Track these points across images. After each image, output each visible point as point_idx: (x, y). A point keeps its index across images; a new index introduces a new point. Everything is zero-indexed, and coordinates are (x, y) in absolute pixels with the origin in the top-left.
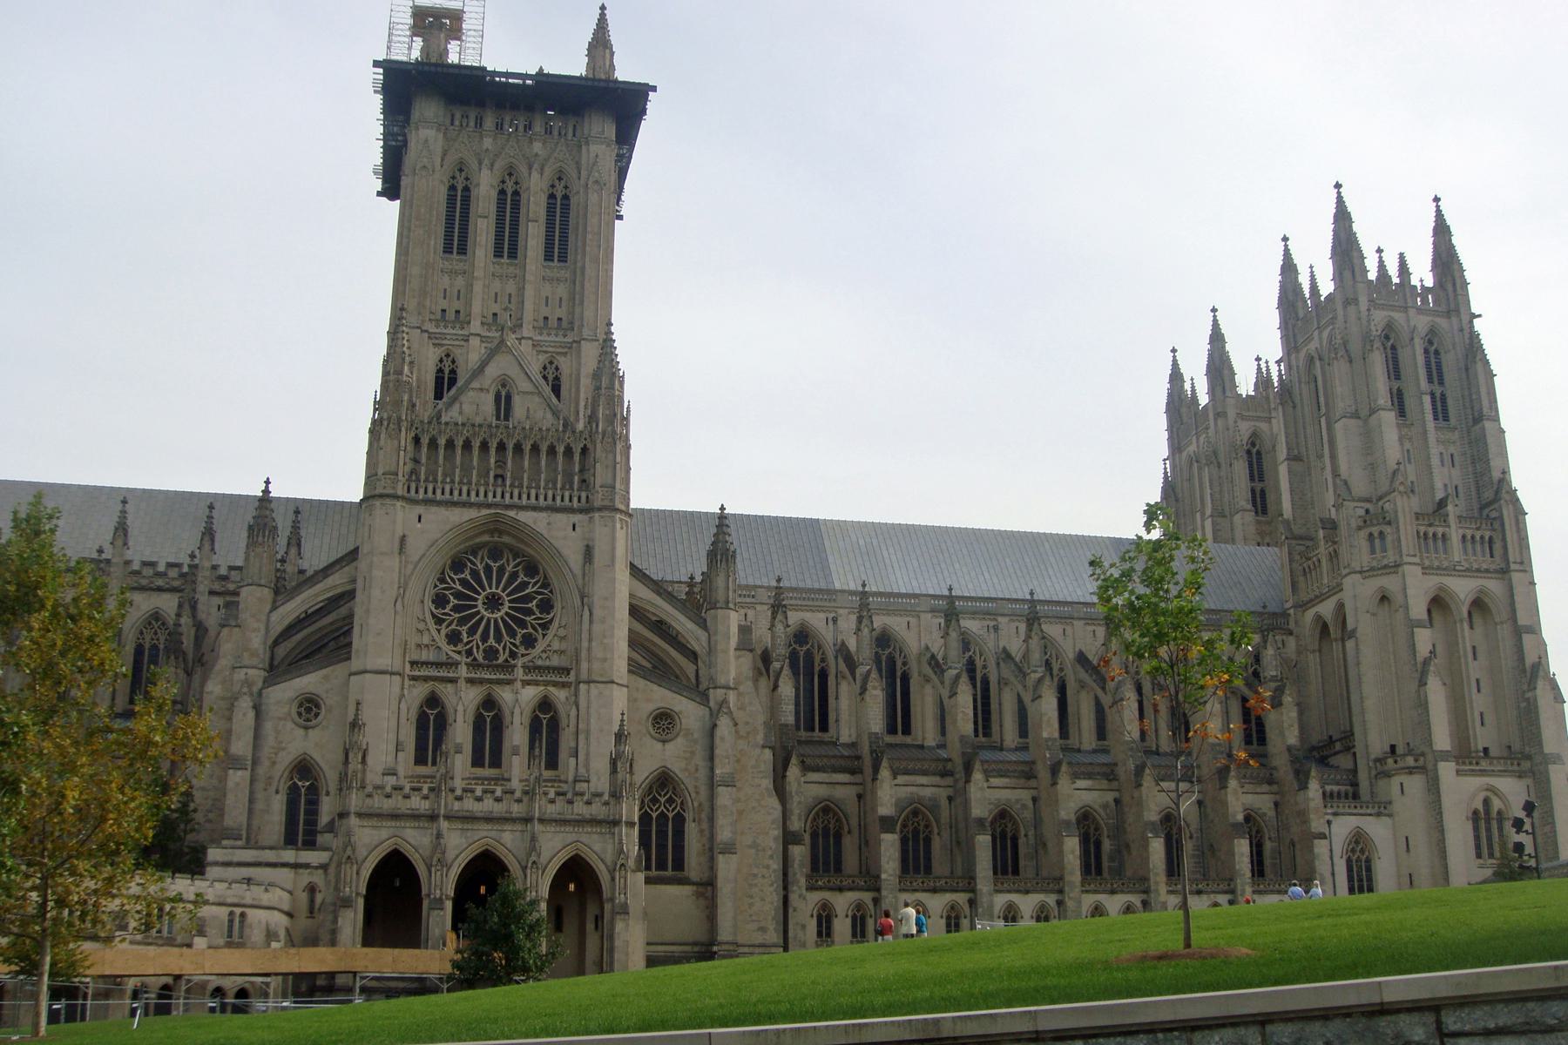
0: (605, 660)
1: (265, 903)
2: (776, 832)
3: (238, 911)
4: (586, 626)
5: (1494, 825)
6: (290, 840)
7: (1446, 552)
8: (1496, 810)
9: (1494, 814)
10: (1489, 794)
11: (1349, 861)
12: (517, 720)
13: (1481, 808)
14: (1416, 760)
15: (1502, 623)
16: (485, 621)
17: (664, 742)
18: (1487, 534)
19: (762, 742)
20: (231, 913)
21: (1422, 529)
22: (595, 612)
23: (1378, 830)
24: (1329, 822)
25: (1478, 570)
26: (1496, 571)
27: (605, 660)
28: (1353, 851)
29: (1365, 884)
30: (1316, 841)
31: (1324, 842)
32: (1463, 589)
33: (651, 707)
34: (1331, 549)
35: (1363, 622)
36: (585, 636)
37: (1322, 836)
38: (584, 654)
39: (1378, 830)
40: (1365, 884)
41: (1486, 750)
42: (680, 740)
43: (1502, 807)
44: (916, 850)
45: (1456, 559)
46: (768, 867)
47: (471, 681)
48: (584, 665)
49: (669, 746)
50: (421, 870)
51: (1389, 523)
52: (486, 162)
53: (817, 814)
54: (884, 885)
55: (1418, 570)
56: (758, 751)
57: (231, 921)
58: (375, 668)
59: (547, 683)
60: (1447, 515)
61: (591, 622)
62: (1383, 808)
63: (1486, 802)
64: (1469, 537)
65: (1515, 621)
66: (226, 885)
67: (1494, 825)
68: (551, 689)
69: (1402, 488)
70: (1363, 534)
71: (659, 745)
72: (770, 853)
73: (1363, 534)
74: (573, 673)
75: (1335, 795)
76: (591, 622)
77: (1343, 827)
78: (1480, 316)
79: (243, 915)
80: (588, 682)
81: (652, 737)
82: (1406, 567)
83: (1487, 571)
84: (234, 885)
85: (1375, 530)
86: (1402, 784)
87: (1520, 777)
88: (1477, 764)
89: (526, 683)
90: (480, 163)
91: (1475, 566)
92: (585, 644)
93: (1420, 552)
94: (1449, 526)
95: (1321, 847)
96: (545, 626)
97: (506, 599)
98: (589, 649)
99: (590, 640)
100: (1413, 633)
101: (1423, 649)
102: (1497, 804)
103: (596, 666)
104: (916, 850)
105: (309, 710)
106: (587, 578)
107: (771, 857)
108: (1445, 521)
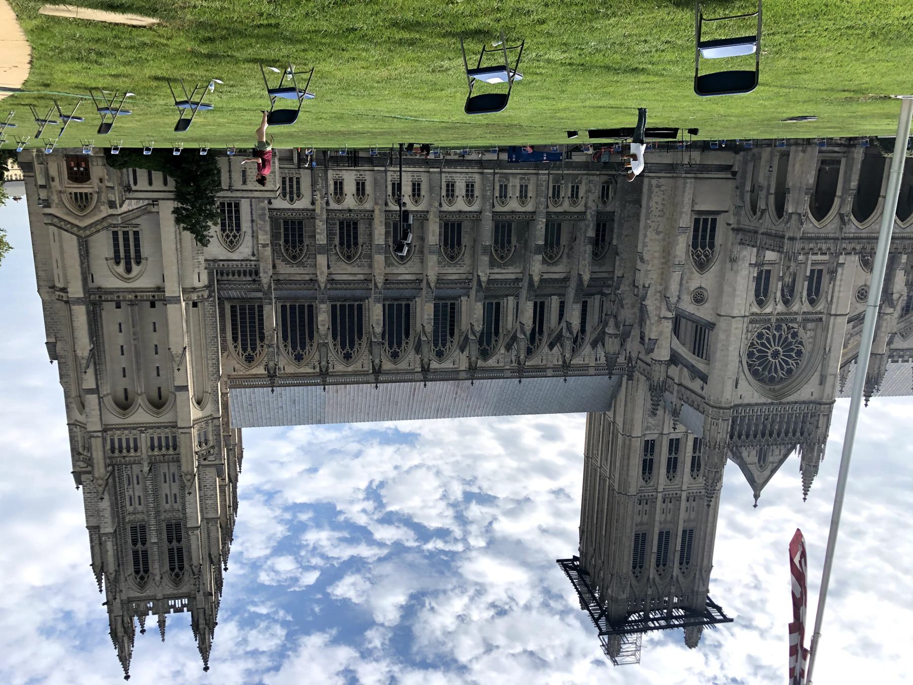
5: (122, 254)
9: (123, 262)
10: (126, 276)
11: (238, 230)
13: (134, 265)
15: (108, 394)
17: (701, 288)
21: (171, 452)
28: (235, 236)
32: (142, 415)
33: (707, 305)
41: (118, 307)
42: (692, 289)
43: (115, 267)
44: (503, 236)
47: (821, 313)
49: (698, 285)
52: (675, 579)
53: (556, 256)
54: (544, 215)
59: (761, 314)
63: (129, 270)
65: (99, 398)
67: (122, 254)
68: (759, 312)
71: (703, 286)
75: (248, 274)
80: (745, 316)
81: (706, 290)
89: (796, 313)
90: (677, 579)
104: (503, 236)
105: (862, 294)
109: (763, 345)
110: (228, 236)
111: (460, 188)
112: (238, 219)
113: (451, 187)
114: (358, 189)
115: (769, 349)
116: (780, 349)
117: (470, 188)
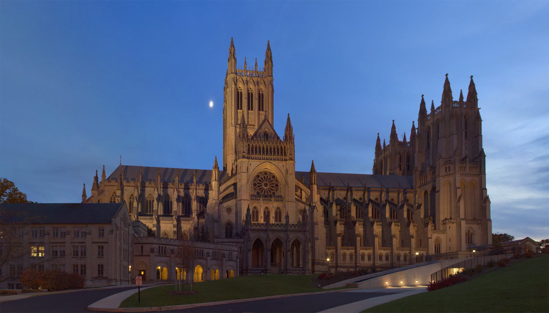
0: (291, 197)
1: (235, 250)
2: (325, 236)
3: (231, 252)
4: (287, 189)
6: (227, 237)
7: (465, 171)
8: (471, 232)
12: (273, 211)
13: (467, 232)
14: (454, 221)
18: (476, 165)
19: (322, 216)
20: (229, 252)
22: (289, 185)
23: (442, 237)
24: (432, 235)
25: (473, 175)
26: (477, 175)
27: (291, 197)
29: (438, 249)
30: (429, 239)
31: (431, 239)
36: (287, 191)
37: (431, 238)
38: (287, 195)
39: (442, 237)
40: (438, 249)
45: (468, 172)
46: (323, 243)
48: (287, 198)
50: (264, 243)
51: (452, 163)
55: (459, 174)
56: (321, 217)
57: (229, 254)
58: (244, 199)
60: (466, 161)
61: (288, 188)
62: (444, 232)
64: (471, 167)
66: (228, 246)
69: (457, 154)
72: (323, 240)
76: (288, 188)
77: (435, 236)
78: (480, 108)
79: (231, 253)
82: (456, 174)
83: (475, 175)
84: (230, 246)
86: (450, 226)
87: (478, 225)
88: (468, 222)
91: (472, 174)
92: (287, 193)
93: (460, 171)
94: (467, 164)
95: (430, 240)
97: (269, 184)
98: (288, 194)
99: (288, 192)
100: (457, 190)
101: (458, 195)
102: (471, 231)
103: (290, 198)
107: (324, 241)
108: (466, 163)
109: (259, 186)
110: (438, 242)
111: (366, 258)
112: (435, 248)
113: (369, 259)
114: (399, 258)
116: (264, 187)
117: (363, 259)
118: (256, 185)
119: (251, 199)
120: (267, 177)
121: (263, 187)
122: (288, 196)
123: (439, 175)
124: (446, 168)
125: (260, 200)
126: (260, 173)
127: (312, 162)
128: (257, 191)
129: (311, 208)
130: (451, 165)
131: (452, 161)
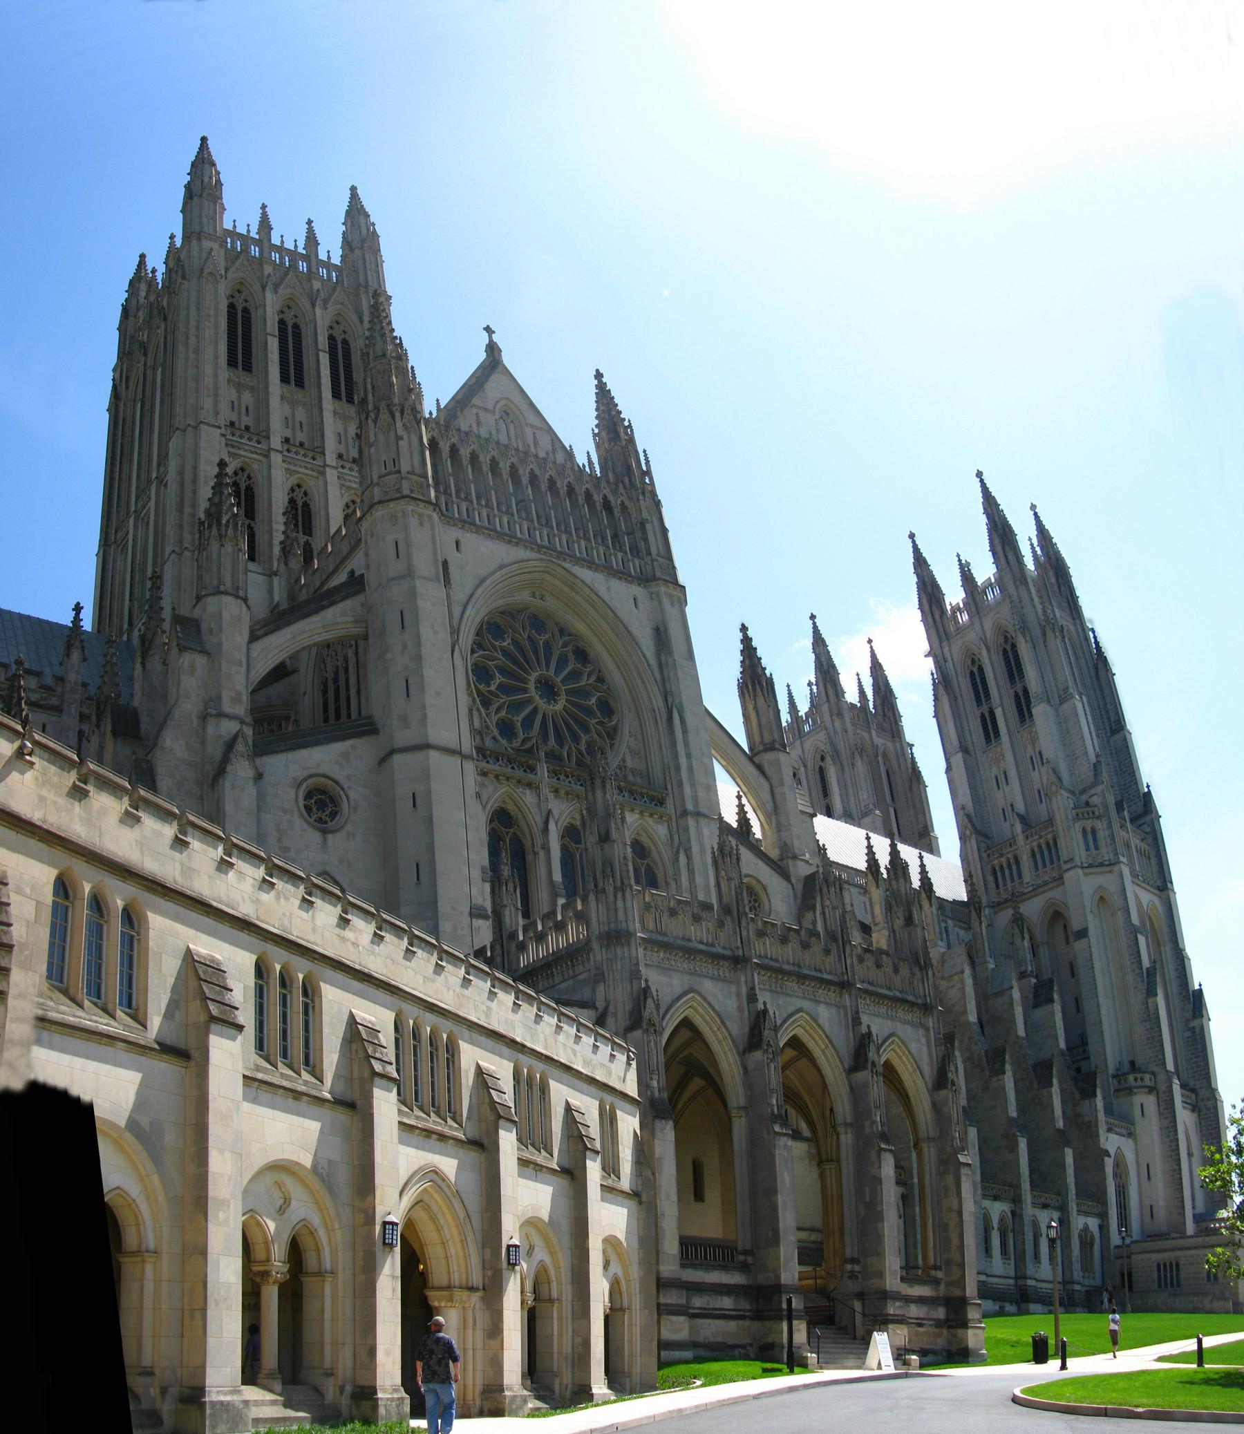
16: (531, 707)
34: (1035, 844)
35: (1085, 914)
70: (1078, 826)
73: (1078, 826)
74: (669, 802)
76: (685, 731)
85: (1089, 824)
96: (612, 734)
98: (690, 769)
106: (665, 672)
115: (535, 710)
118: (492, 677)
119: (482, 752)
120: (547, 645)
121: (529, 701)
122: (693, 785)
123: (1072, 859)
124: (1084, 831)
125: (532, 769)
126: (503, 613)
127: (740, 635)
128: (503, 713)
129: (793, 885)
130: (1099, 825)
131: (1096, 806)
